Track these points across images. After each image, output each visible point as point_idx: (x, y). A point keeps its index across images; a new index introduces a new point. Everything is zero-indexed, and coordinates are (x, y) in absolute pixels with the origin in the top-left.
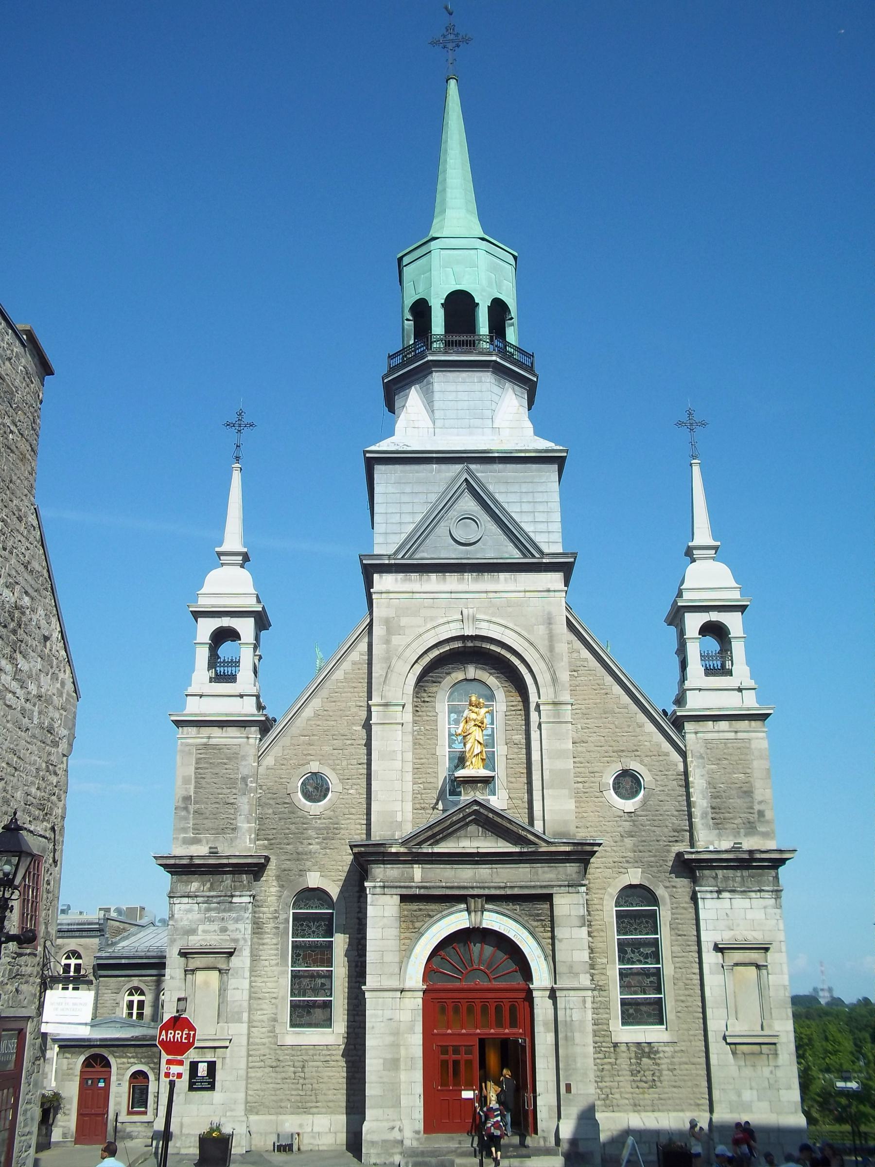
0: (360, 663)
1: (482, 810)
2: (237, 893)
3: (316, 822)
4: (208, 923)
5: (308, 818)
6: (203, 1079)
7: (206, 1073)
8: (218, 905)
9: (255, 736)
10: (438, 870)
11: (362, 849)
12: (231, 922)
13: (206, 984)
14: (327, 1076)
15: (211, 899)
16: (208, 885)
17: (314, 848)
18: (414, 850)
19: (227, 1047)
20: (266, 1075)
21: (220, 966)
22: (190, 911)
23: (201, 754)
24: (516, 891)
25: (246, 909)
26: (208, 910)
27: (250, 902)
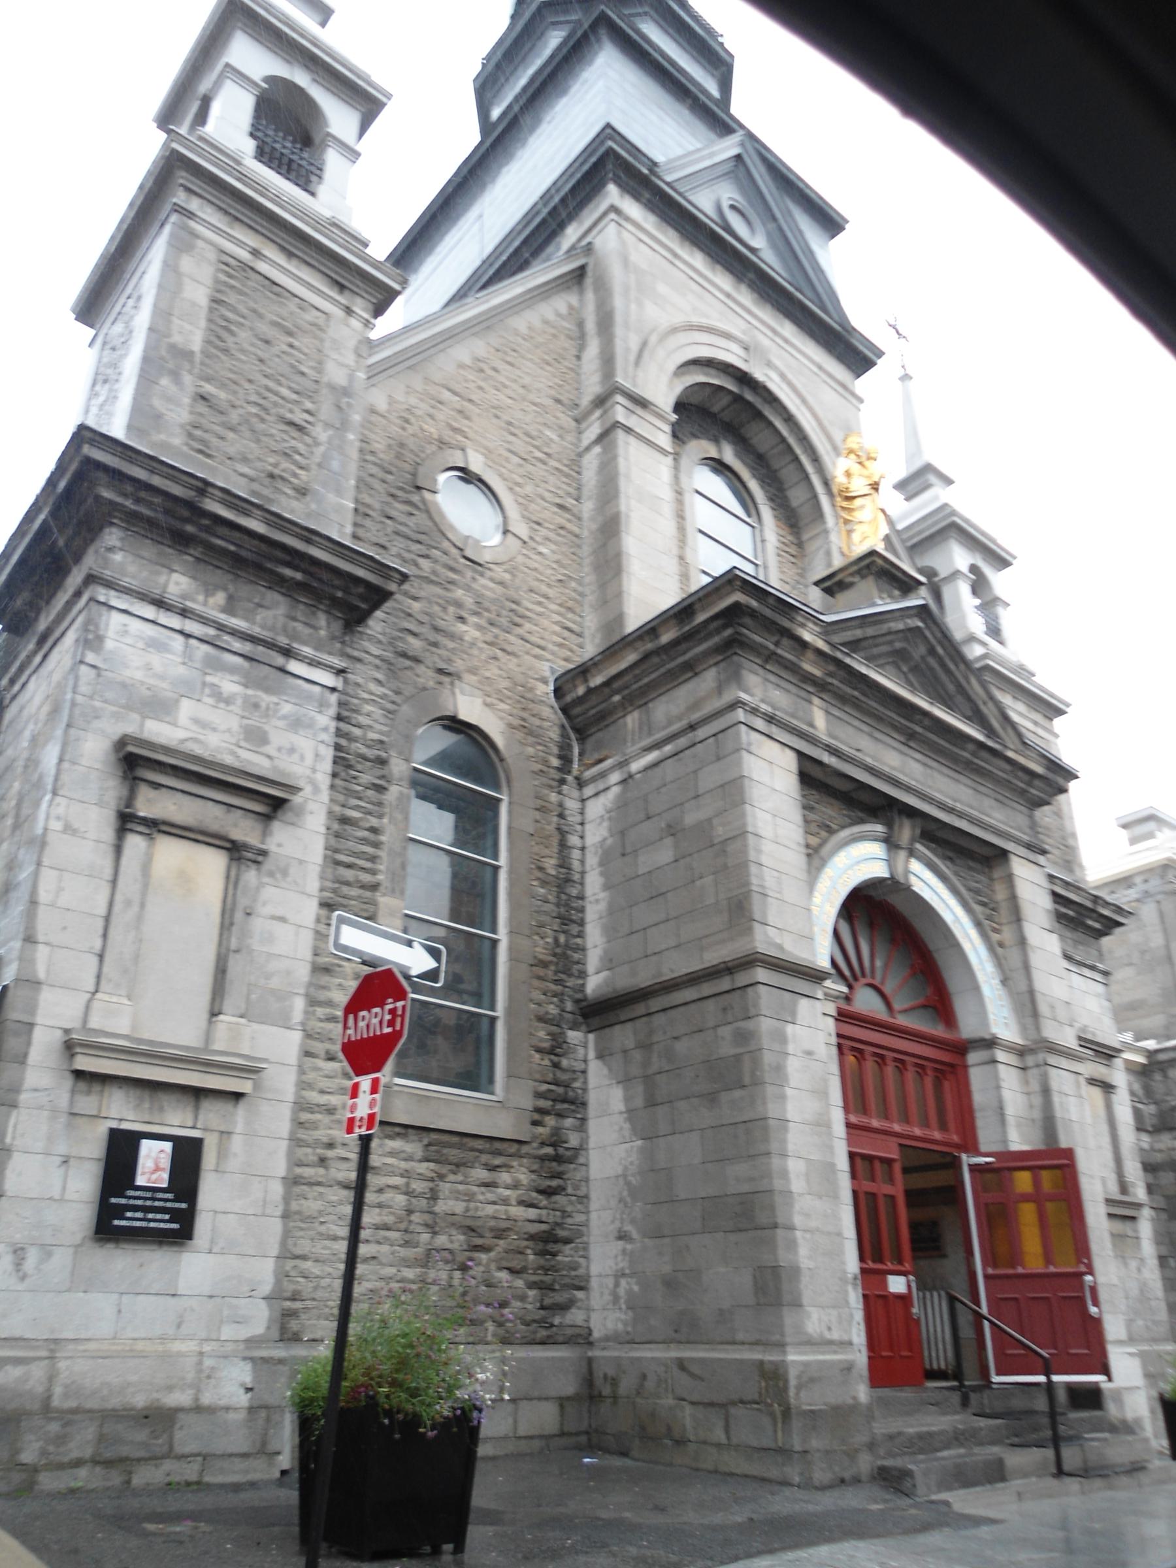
2: (307, 650)
3: (474, 579)
4: (210, 701)
9: (366, 316)
10: (851, 730)
12: (281, 724)
13: (184, 878)
14: (492, 1230)
15: (226, 637)
16: (220, 598)
17: (469, 632)
18: (839, 655)
19: (238, 1096)
21: (237, 835)
23: (230, 276)
25: (322, 705)
26: (212, 665)
27: (333, 690)
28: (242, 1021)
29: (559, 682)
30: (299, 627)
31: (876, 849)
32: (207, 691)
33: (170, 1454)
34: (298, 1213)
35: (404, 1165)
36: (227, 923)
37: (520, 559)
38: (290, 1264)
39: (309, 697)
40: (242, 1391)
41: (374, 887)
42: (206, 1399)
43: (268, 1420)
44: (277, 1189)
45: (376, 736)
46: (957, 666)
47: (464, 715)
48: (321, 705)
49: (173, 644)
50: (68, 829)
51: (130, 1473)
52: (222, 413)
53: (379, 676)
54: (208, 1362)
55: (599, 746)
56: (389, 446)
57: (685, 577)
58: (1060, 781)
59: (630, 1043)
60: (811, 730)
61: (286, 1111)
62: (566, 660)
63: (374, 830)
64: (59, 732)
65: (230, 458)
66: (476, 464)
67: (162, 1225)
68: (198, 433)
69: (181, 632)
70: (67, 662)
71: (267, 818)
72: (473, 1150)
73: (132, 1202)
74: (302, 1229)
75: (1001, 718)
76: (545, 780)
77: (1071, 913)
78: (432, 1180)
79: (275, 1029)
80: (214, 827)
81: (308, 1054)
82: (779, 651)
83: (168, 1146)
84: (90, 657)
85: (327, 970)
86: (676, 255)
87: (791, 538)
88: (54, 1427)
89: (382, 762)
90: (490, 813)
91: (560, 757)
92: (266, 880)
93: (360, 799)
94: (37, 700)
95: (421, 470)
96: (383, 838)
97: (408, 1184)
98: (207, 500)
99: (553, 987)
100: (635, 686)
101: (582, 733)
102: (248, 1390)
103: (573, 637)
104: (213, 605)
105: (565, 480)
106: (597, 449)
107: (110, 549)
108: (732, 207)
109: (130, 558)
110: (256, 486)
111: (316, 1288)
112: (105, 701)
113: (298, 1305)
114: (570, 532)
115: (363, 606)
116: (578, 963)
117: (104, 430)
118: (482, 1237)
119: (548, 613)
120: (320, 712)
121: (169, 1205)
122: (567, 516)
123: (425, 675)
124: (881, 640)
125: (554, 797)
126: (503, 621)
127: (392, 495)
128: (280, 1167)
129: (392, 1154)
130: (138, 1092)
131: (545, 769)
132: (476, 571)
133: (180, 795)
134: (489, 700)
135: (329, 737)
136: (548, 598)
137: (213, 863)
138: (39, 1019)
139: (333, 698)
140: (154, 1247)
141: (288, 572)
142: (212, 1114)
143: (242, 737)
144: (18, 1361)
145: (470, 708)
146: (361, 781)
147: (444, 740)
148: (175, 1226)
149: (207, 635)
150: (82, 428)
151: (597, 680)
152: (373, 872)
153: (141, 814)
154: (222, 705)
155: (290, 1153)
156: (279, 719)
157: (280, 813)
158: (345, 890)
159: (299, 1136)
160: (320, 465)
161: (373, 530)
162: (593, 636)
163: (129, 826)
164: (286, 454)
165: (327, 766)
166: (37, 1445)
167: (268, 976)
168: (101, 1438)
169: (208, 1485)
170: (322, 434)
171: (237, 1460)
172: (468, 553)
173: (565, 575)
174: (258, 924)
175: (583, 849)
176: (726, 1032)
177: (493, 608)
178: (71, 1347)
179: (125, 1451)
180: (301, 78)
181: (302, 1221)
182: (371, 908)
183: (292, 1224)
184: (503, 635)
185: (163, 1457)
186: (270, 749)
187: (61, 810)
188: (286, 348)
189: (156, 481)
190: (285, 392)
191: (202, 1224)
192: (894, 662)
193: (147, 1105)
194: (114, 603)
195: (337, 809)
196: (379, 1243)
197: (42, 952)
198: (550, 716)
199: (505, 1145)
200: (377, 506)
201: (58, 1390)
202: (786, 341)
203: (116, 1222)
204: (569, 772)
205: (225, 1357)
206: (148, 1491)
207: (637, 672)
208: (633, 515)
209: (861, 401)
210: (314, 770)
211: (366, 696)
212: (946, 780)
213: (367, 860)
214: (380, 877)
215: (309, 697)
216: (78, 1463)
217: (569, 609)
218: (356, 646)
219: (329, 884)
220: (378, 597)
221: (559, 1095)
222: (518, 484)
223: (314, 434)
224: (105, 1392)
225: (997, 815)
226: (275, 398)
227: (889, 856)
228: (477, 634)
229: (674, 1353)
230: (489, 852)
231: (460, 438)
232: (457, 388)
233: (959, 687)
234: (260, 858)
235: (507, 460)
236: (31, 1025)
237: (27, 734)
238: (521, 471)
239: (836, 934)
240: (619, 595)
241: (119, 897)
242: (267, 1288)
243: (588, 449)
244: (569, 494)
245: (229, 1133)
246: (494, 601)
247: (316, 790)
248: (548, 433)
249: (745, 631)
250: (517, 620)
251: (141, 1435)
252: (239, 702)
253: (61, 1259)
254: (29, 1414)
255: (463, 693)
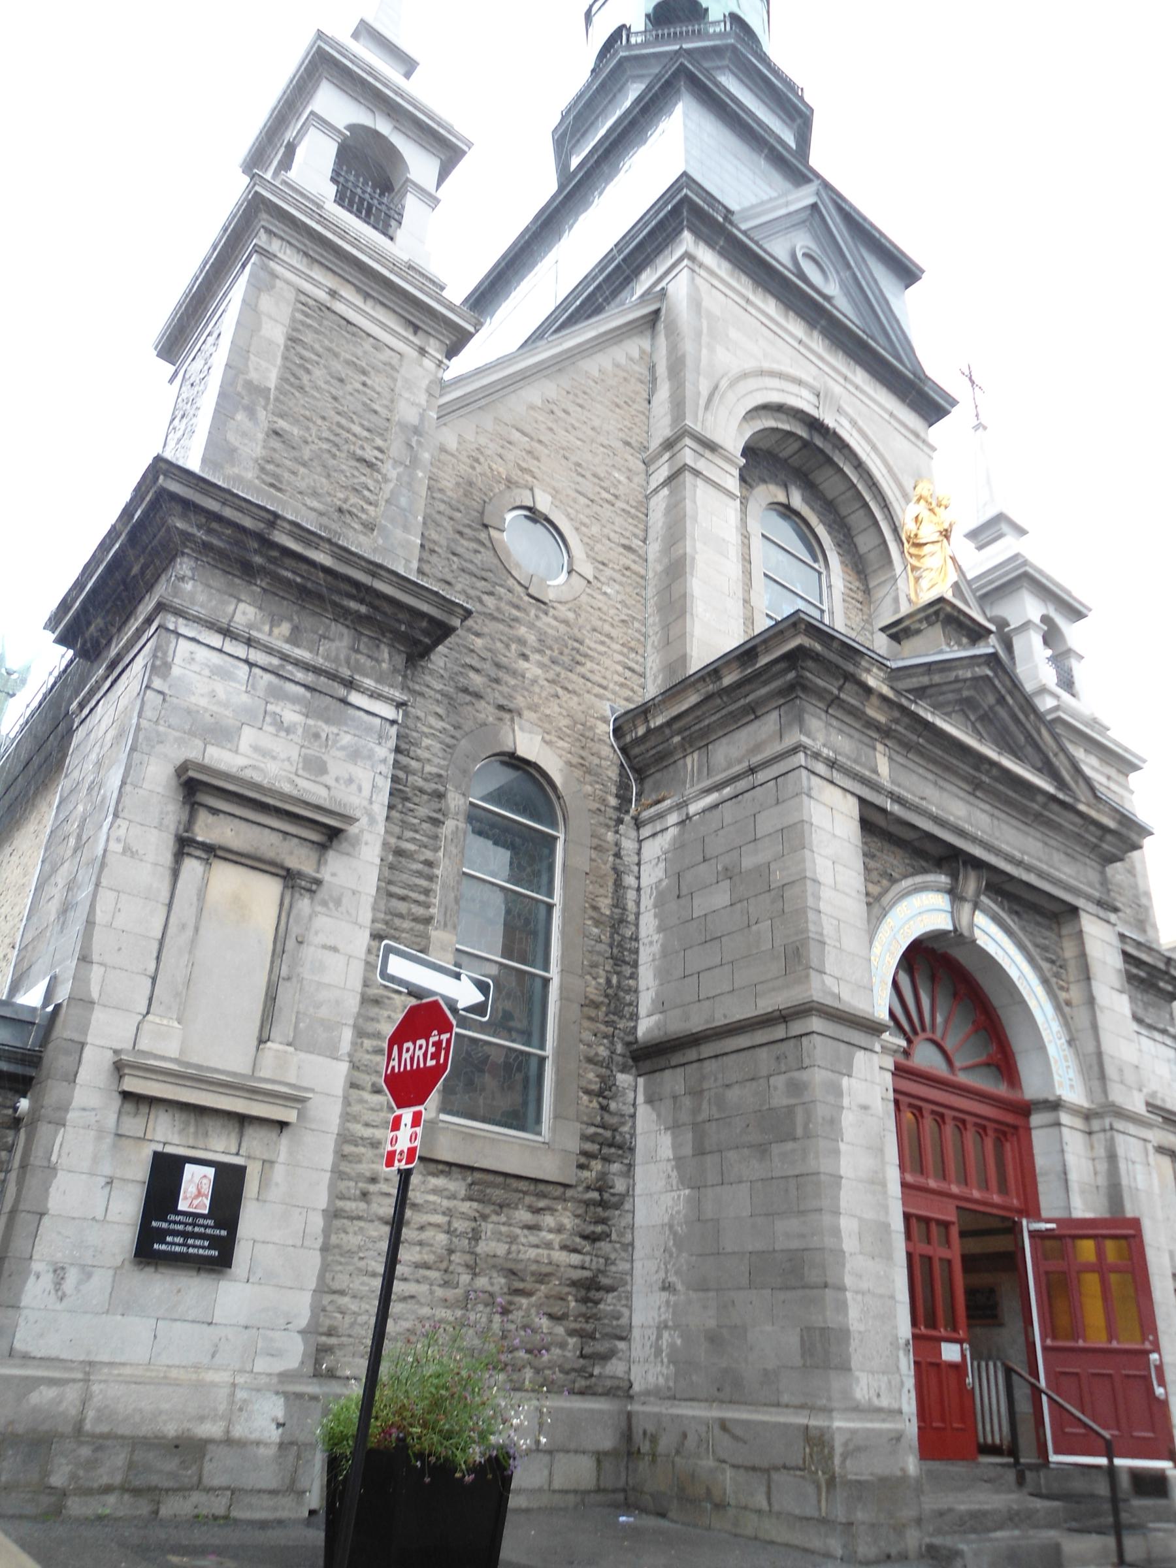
0: (627, 372)
1: (997, 682)
2: (369, 683)
3: (537, 616)
4: (272, 729)
5: (521, 599)
6: (194, 1225)
7: (207, 1203)
8: (308, 695)
9: (440, 357)
10: (914, 778)
11: (818, 647)
14: (533, 1274)
15: (290, 667)
16: (285, 628)
17: (531, 669)
19: (282, 1125)
20: (370, 1245)
21: (292, 863)
22: (218, 673)
23: (307, 315)
24: (1032, 879)
25: (381, 737)
26: (275, 694)
27: (393, 722)
28: (291, 1049)
29: (617, 724)
30: (362, 659)
31: (941, 901)
32: (268, 719)
33: (199, 1486)
34: (338, 1246)
35: (446, 1203)
36: (279, 951)
37: (584, 598)
38: (326, 1299)
39: (369, 729)
40: (274, 1426)
41: (428, 921)
42: (238, 1432)
43: (298, 1457)
44: (317, 1222)
45: (434, 770)
46: (1027, 716)
47: (522, 752)
48: (380, 737)
49: (237, 672)
50: (127, 850)
51: (159, 1503)
52: (293, 448)
53: (440, 710)
54: (241, 1395)
55: (657, 787)
56: (458, 484)
57: (749, 620)
58: (1134, 837)
59: (680, 1088)
60: (874, 776)
61: (330, 1143)
62: (627, 699)
63: (429, 864)
64: (123, 757)
65: (300, 493)
66: (544, 504)
67: (201, 1252)
68: (270, 467)
69: (246, 661)
70: (135, 687)
71: (323, 847)
72: (517, 1191)
73: (172, 1226)
74: (341, 1263)
75: (1072, 771)
76: (602, 819)
77: (1142, 974)
78: (475, 1219)
79: (321, 1059)
80: (270, 854)
81: (353, 1085)
82: (842, 696)
83: (210, 1172)
84: (157, 683)
85: (377, 1002)
86: (748, 301)
87: (857, 584)
88: (85, 1452)
89: (440, 796)
90: (546, 851)
91: (617, 796)
92: (319, 909)
93: (416, 831)
94: (103, 727)
95: (488, 508)
96: (438, 872)
97: (449, 1223)
98: (276, 532)
99: (603, 1028)
100: (697, 727)
101: (641, 774)
102: (280, 1425)
103: (635, 677)
104: (278, 636)
105: (630, 520)
106: (665, 491)
107: (182, 579)
108: (805, 255)
109: (200, 588)
110: (324, 520)
111: (352, 1325)
112: (169, 727)
113: (333, 1341)
114: (635, 573)
115: (427, 640)
116: (630, 1004)
117: (180, 463)
118: (523, 1280)
119: (610, 652)
120: (380, 744)
121: (209, 1231)
122: (633, 557)
123: (486, 712)
124: (945, 688)
125: (610, 836)
126: (566, 659)
127: (461, 533)
128: (322, 1200)
129: (435, 1191)
130: (184, 1116)
131: (603, 808)
132: (539, 609)
133: (237, 821)
134: (547, 737)
135: (387, 769)
136: (612, 638)
137: (267, 890)
138: (89, 1039)
139: (393, 730)
140: (194, 1273)
141: (353, 605)
142: (256, 1142)
143: (300, 766)
144: (52, 1382)
145: (528, 745)
146: (417, 814)
147: (504, 776)
148: (215, 1253)
149: (270, 664)
150: (158, 459)
151: (659, 721)
152: (427, 906)
153: (200, 839)
154: (283, 734)
155: (332, 1186)
156: (338, 749)
157: (335, 842)
158: (397, 922)
159: (341, 1168)
160: (387, 501)
161: (439, 566)
162: (656, 677)
163: (186, 850)
164: (356, 490)
165: (384, 797)
166: (67, 1469)
167: (318, 1006)
168: (131, 1465)
169: (236, 1521)
170: (391, 470)
171: (265, 1497)
172: (531, 591)
173: (628, 615)
174: (310, 953)
175: (639, 889)
176: (779, 1081)
177: (556, 647)
178: (106, 1370)
179: (154, 1480)
180: (384, 127)
181: (341, 1255)
182: (424, 942)
183: (330, 1258)
184: (564, 673)
185: (191, 1489)
186: (328, 779)
187: (122, 832)
188: (361, 387)
189: (228, 513)
190: (357, 429)
191: (242, 1252)
192: (962, 710)
193: (192, 1129)
194: (181, 630)
195: (393, 841)
196: (418, 1281)
197: (96, 972)
198: (608, 756)
199: (550, 1188)
200: (444, 542)
201: (91, 1414)
202: (857, 387)
203: (156, 1246)
204: (627, 812)
205: (258, 1390)
206: (175, 1522)
207: (699, 713)
208: (697, 557)
209: (934, 449)
210: (371, 802)
211: (426, 730)
212: (1013, 831)
213: (420, 893)
214: (433, 911)
215: (369, 729)
216: (107, 1490)
217: (632, 649)
218: (419, 680)
219: (382, 916)
220: (442, 632)
221: (606, 1139)
222: (585, 525)
223: (384, 471)
224: (137, 1418)
225: (1067, 870)
226: (345, 434)
227: (952, 907)
228: (539, 672)
229: (715, 1413)
230: (544, 889)
231: (530, 479)
232: (528, 429)
233: (1029, 736)
234: (314, 887)
235: (575, 500)
236: (83, 1045)
237: (93, 757)
238: (588, 511)
239: (895, 984)
240: (683, 636)
241: (173, 920)
242: (303, 1321)
243: (656, 491)
244: (635, 535)
245: (272, 1162)
246: (556, 639)
247: (372, 820)
248: (617, 475)
249: (808, 675)
250: (578, 658)
251: (171, 1465)
252: (300, 731)
253: (101, 1280)
254: (62, 1436)
255: (521, 729)
